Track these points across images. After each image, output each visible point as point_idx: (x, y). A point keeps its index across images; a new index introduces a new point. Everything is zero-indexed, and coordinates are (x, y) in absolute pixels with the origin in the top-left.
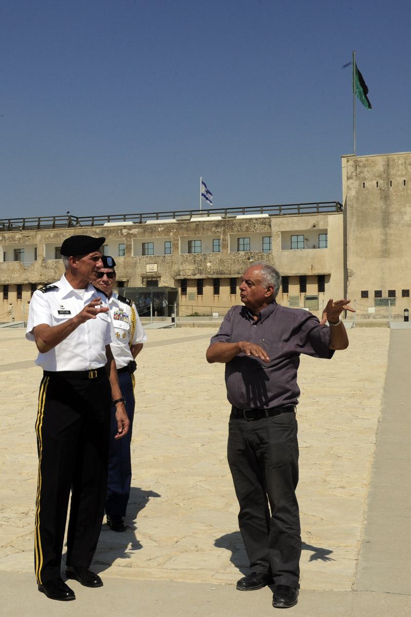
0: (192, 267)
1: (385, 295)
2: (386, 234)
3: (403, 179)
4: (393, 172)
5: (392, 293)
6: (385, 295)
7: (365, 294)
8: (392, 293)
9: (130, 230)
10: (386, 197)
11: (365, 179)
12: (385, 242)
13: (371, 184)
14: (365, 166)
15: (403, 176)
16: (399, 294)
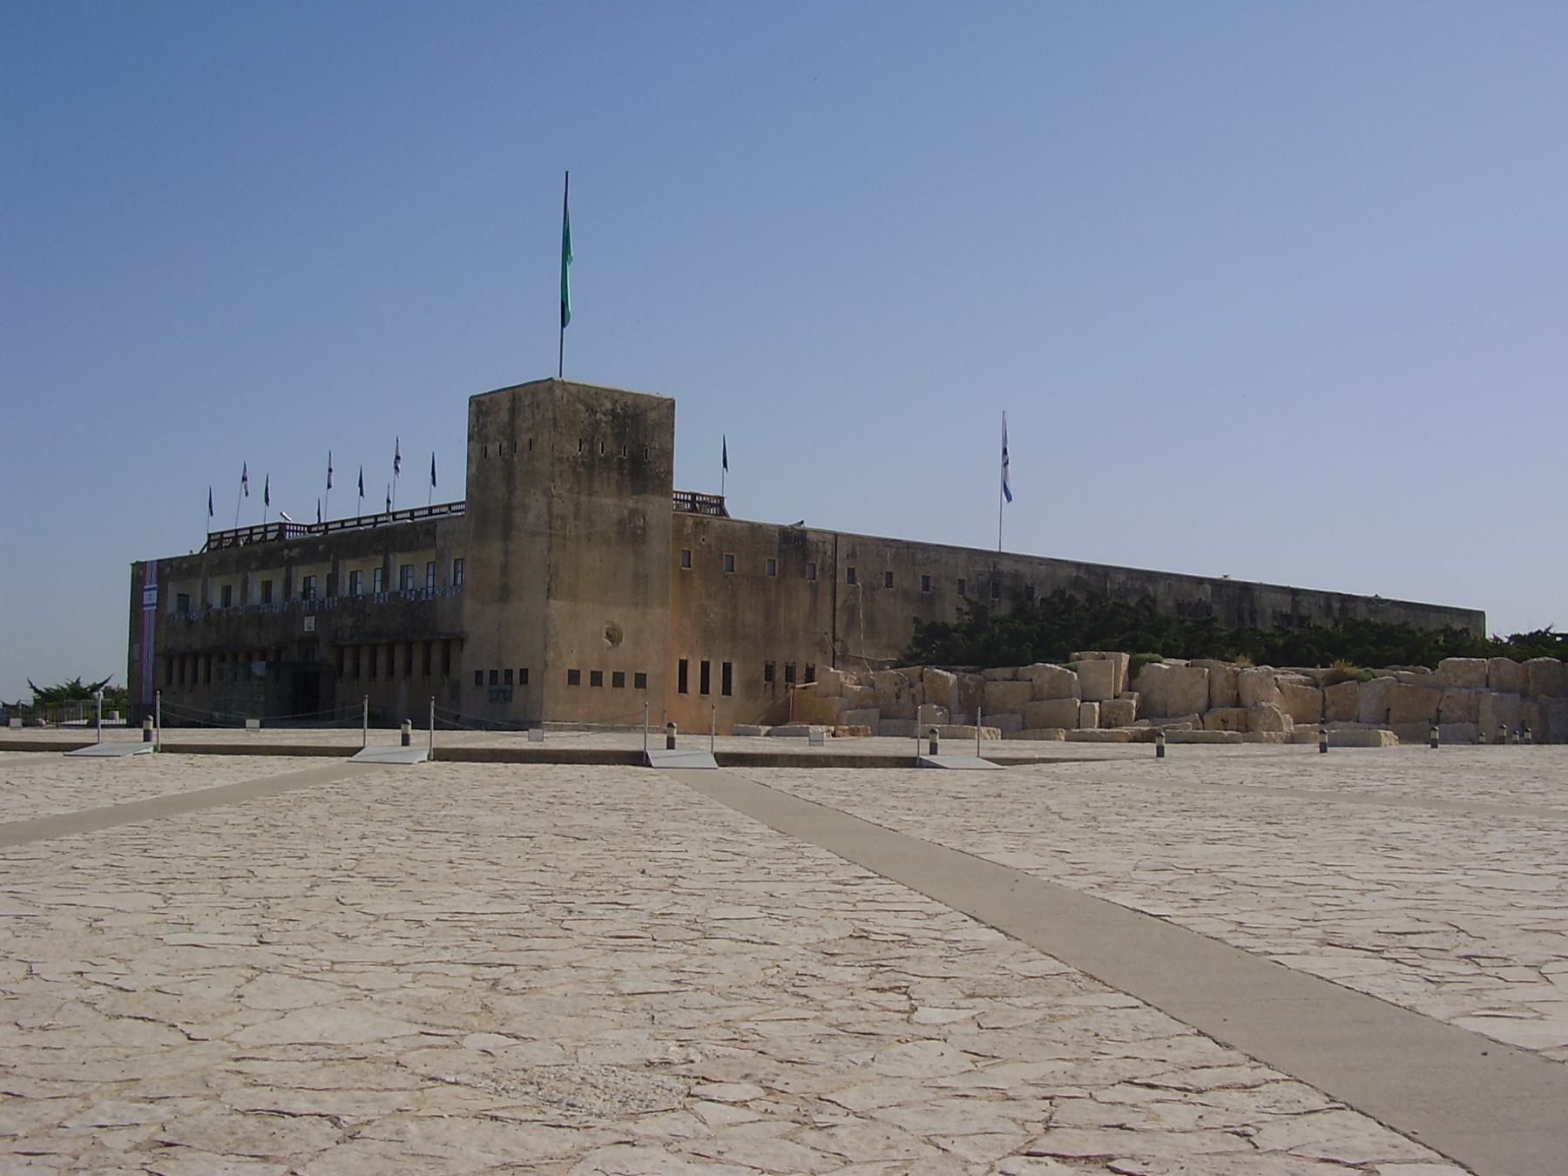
0: (349, 622)
1: (501, 678)
2: (506, 553)
3: (530, 436)
4: (519, 422)
5: (509, 673)
6: (501, 678)
7: (479, 674)
8: (509, 673)
9: (290, 549)
10: (509, 477)
11: (487, 439)
12: (505, 569)
13: (493, 448)
14: (487, 414)
15: (529, 430)
16: (516, 677)
